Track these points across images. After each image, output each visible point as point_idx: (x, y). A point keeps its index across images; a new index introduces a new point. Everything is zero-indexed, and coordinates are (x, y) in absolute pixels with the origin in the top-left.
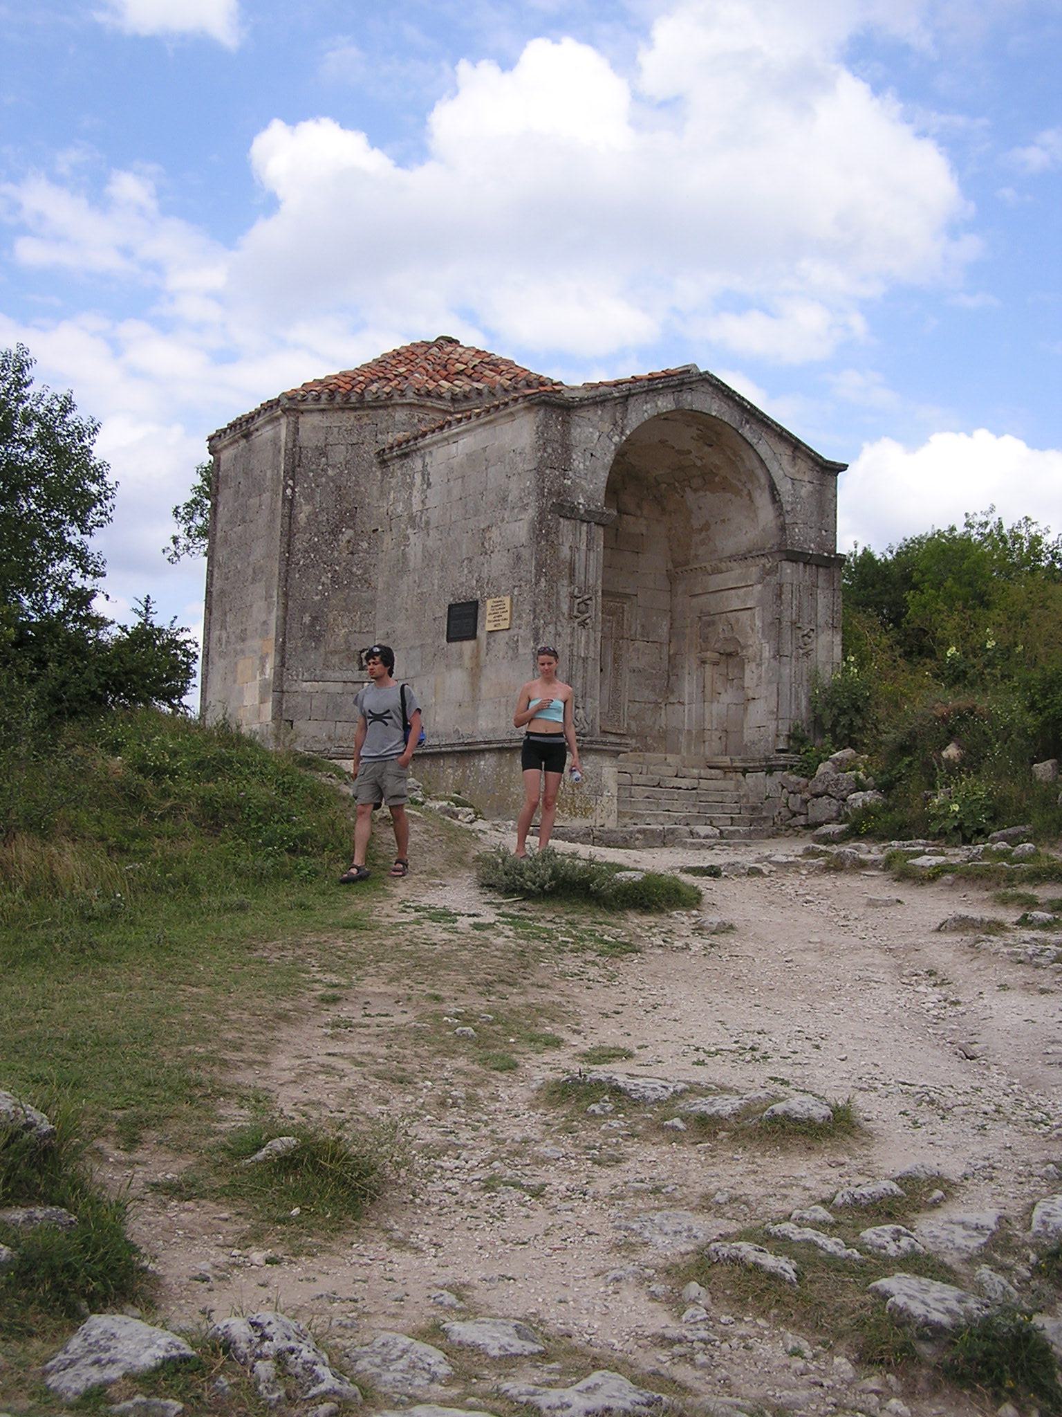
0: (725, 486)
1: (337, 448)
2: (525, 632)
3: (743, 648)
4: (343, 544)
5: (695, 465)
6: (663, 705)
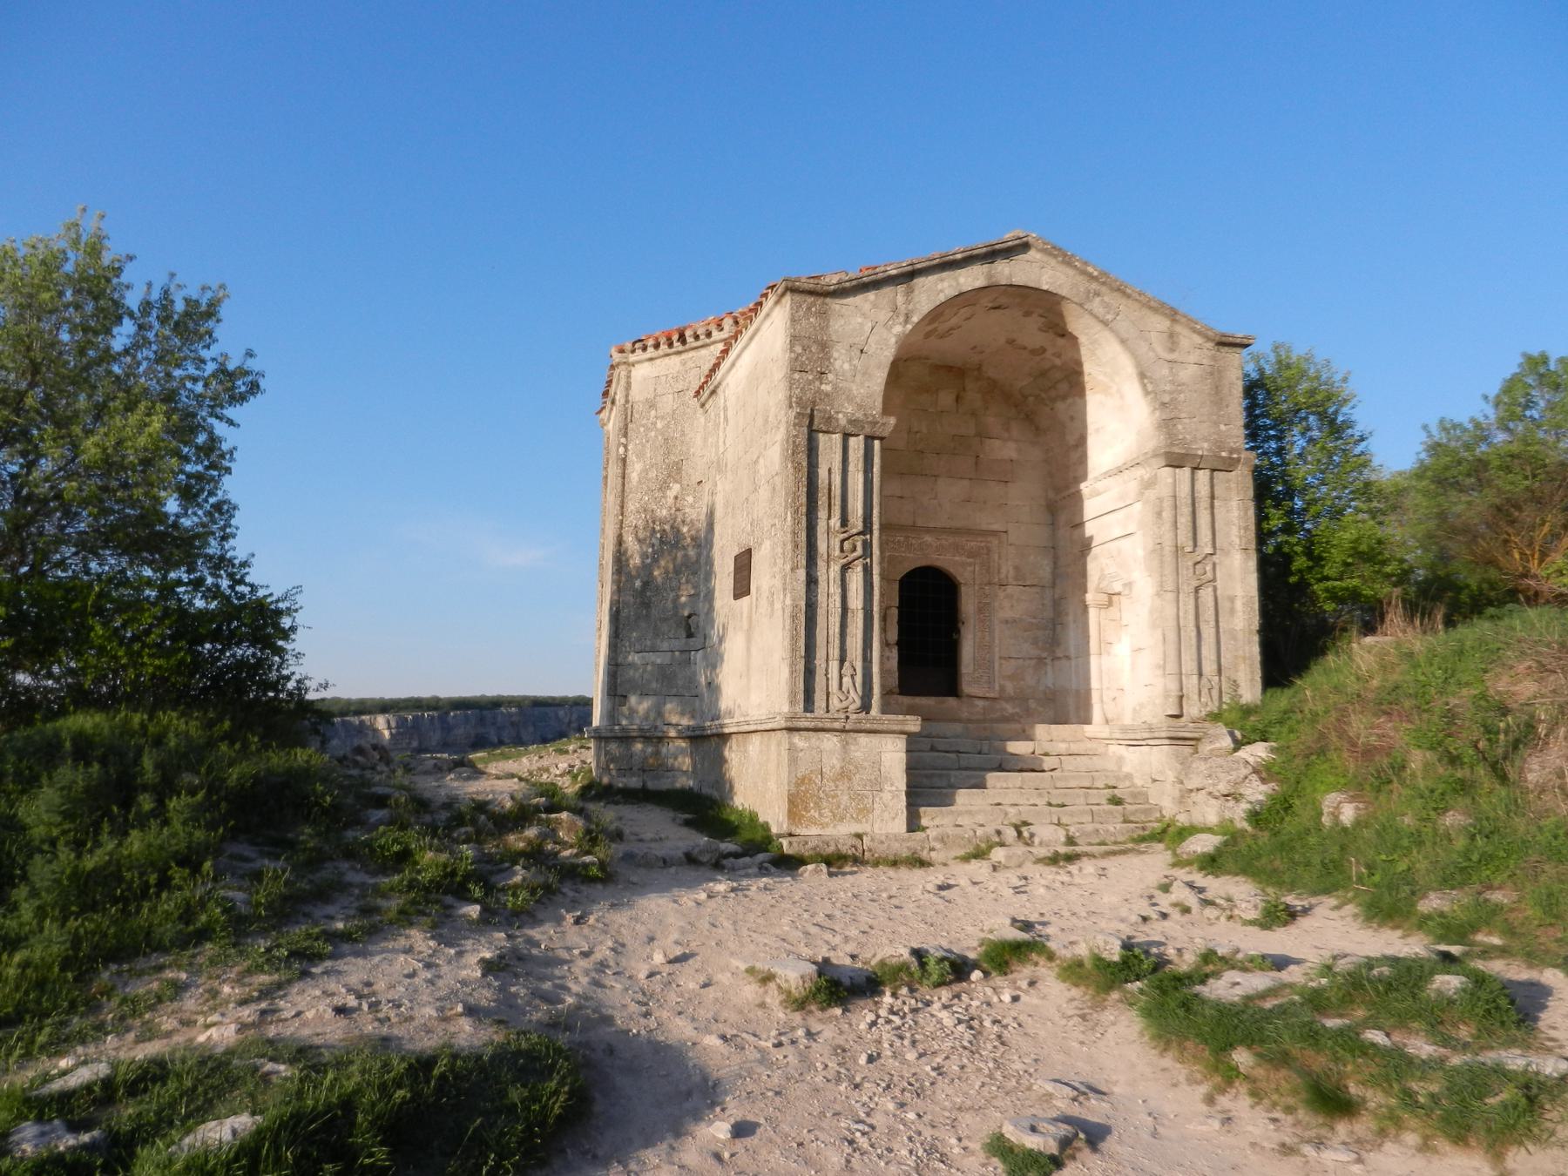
1: (665, 399)
2: (778, 583)
4: (670, 501)
5: (1054, 367)
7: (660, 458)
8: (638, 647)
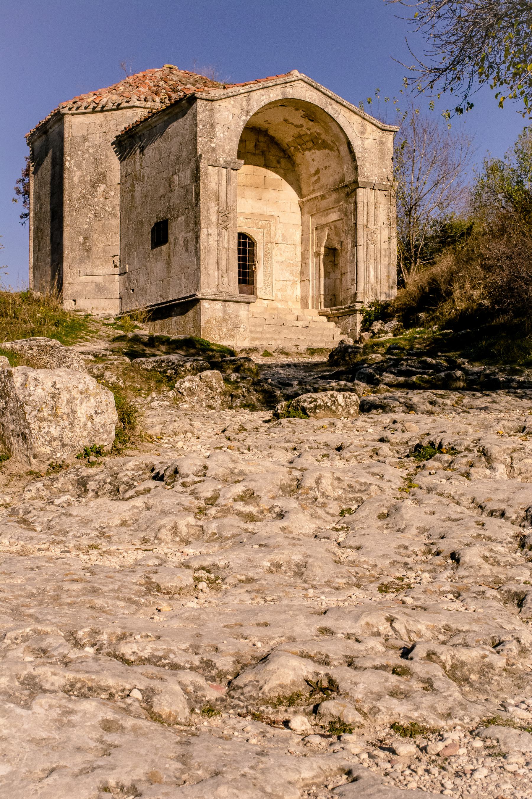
0: (325, 145)
7: (92, 169)
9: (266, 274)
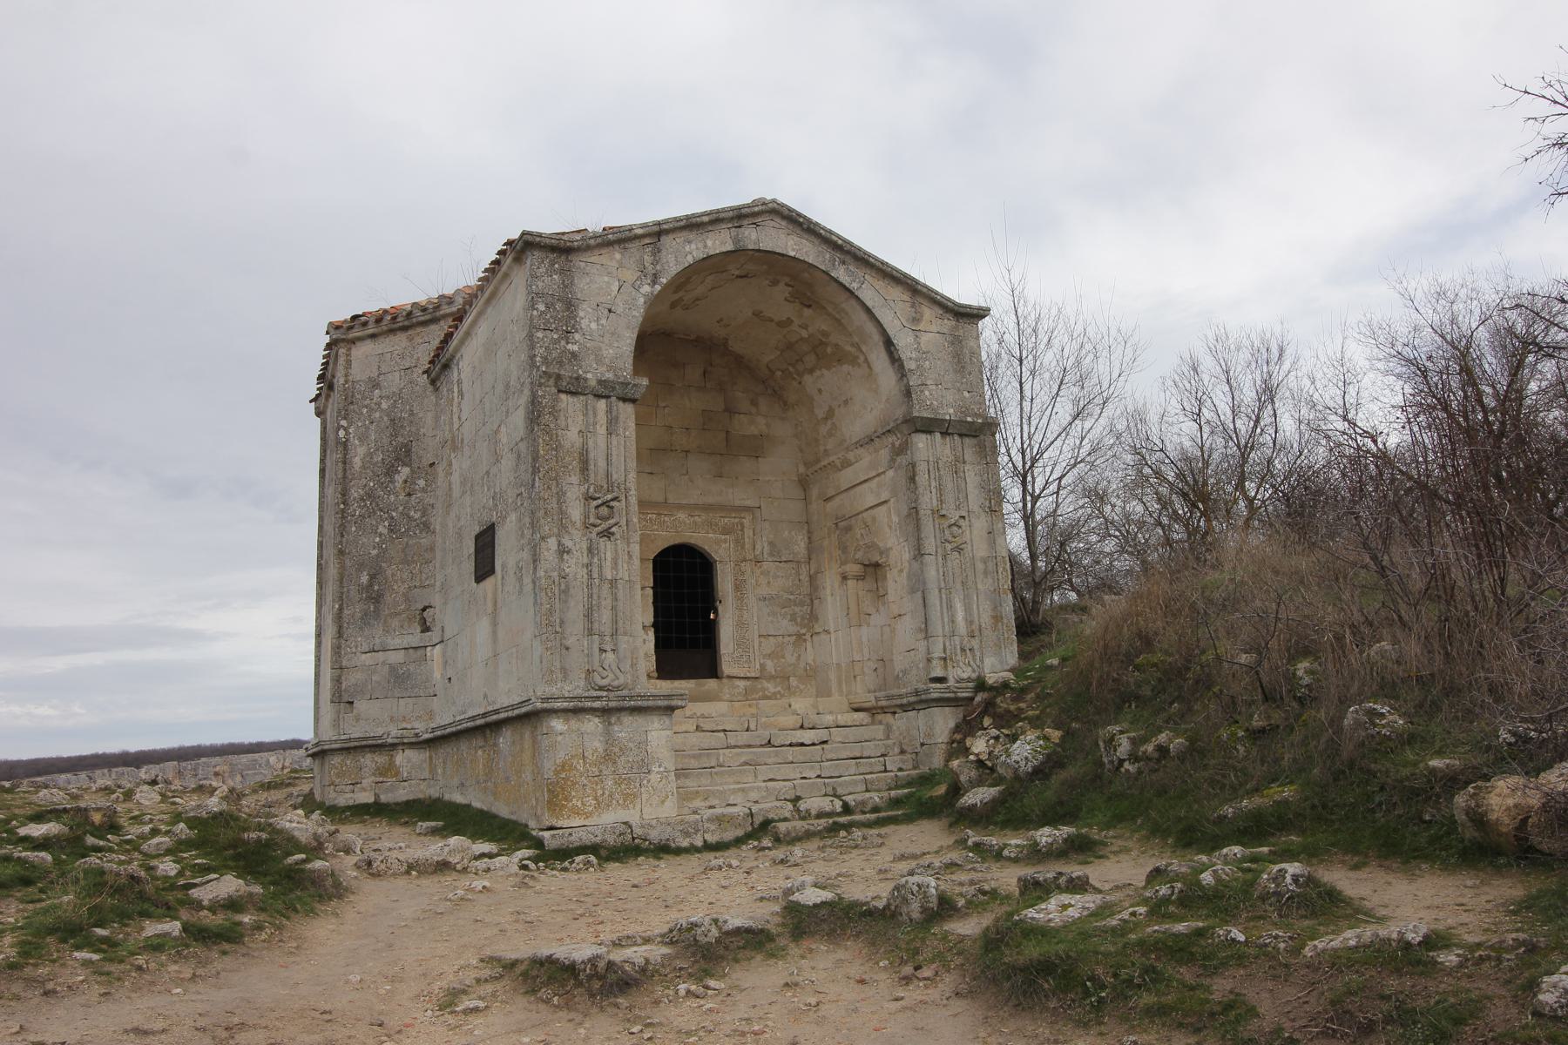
0: (841, 357)
1: (390, 376)
3: (881, 553)
5: (802, 339)
6: (808, 636)
7: (386, 441)
8: (365, 648)
9: (741, 624)
